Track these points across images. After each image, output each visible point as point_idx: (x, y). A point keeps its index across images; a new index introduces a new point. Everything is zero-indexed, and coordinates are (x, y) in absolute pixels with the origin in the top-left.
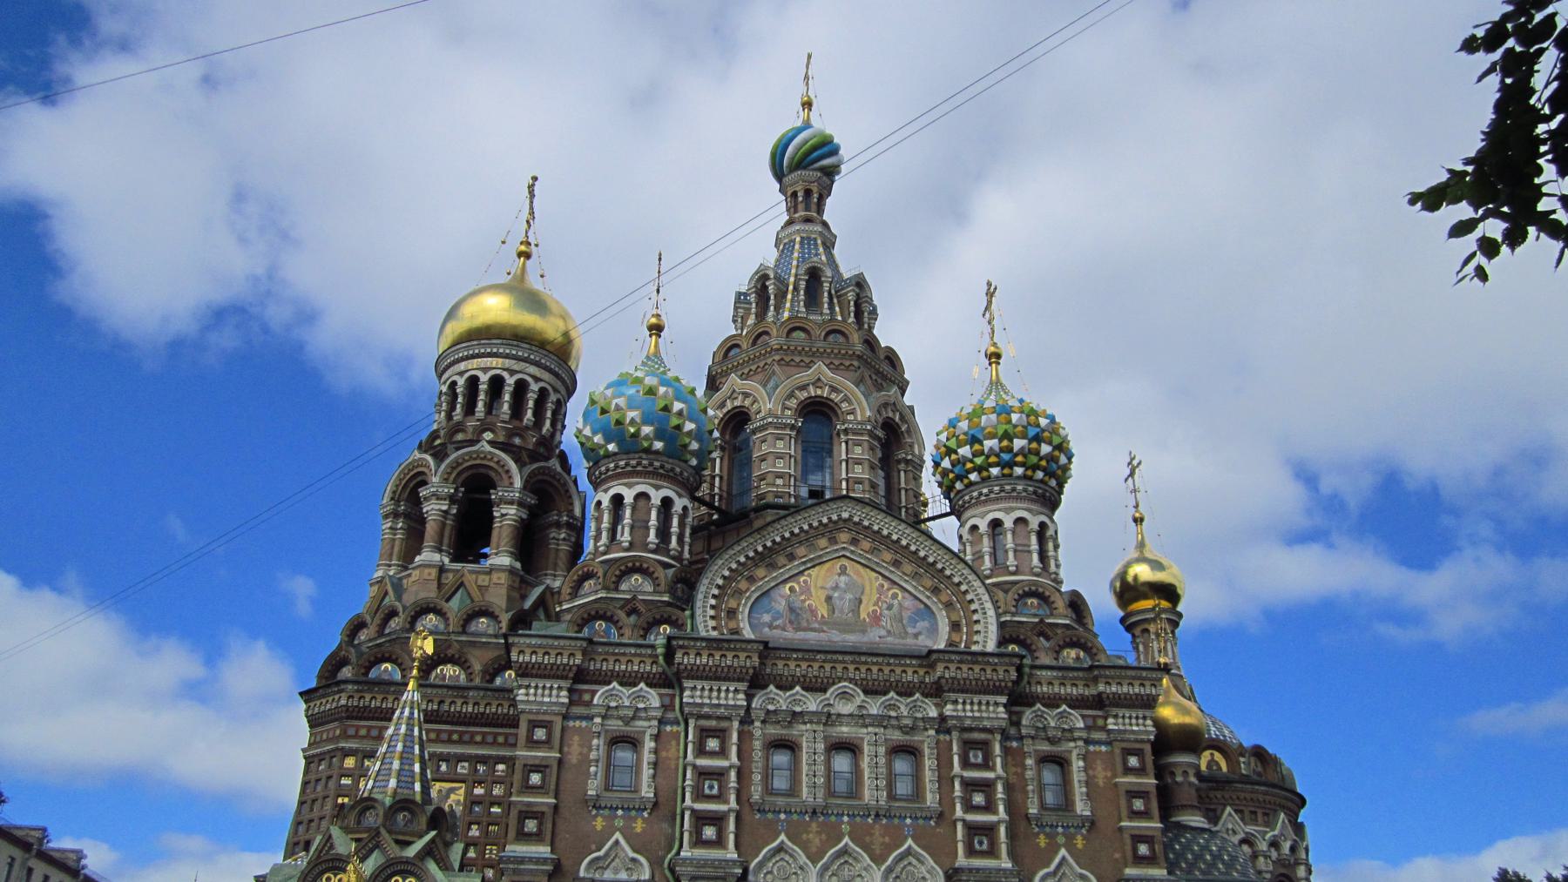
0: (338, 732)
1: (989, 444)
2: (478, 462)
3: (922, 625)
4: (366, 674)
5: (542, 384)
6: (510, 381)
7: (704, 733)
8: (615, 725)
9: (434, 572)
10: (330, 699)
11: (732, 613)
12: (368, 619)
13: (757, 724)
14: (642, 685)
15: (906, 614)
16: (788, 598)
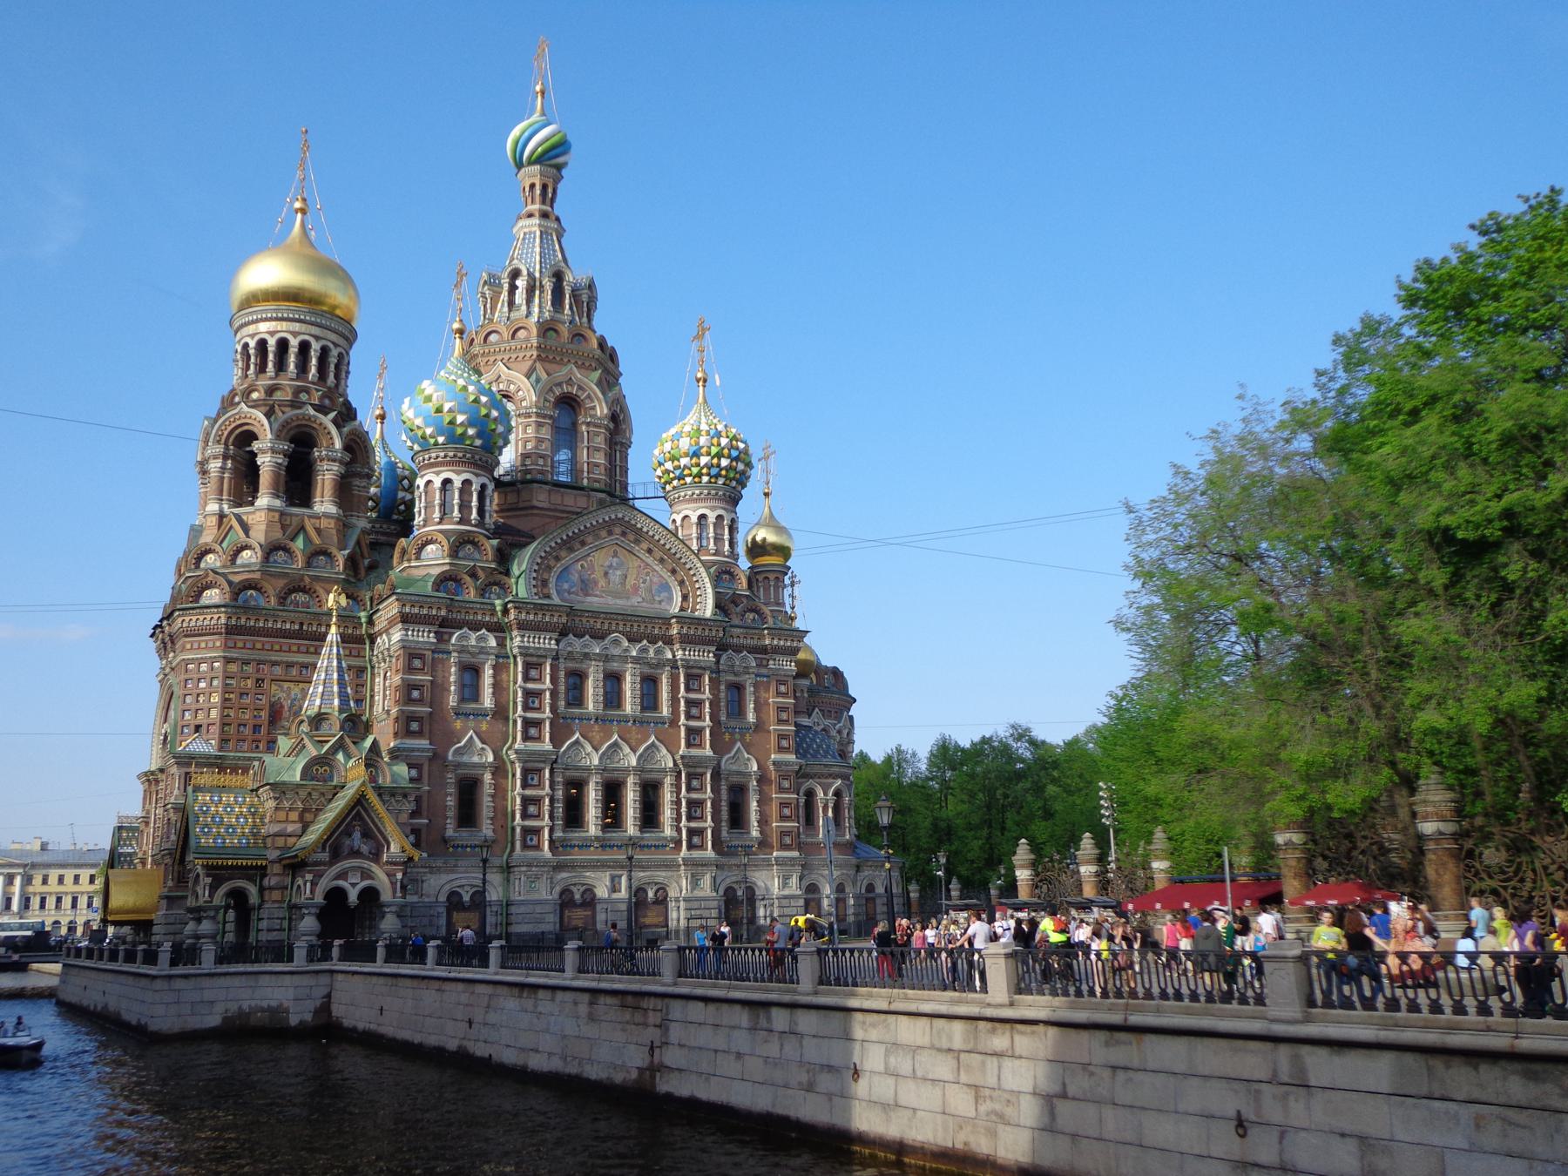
0: (218, 644)
1: (704, 460)
2: (304, 422)
3: (664, 595)
4: (236, 600)
5: (339, 350)
6: (316, 346)
7: (528, 666)
8: (466, 658)
9: (277, 515)
10: (209, 617)
11: (545, 583)
12: (218, 548)
13: (561, 660)
14: (484, 631)
15: (655, 587)
16: (579, 573)
